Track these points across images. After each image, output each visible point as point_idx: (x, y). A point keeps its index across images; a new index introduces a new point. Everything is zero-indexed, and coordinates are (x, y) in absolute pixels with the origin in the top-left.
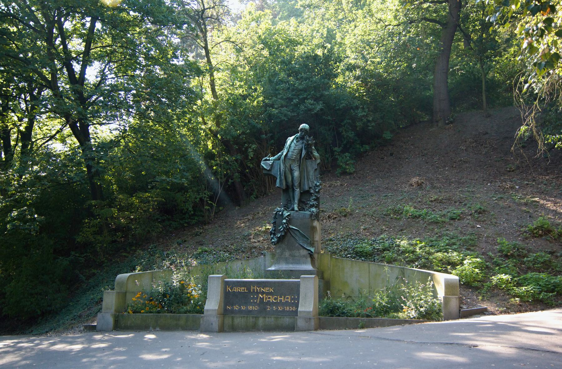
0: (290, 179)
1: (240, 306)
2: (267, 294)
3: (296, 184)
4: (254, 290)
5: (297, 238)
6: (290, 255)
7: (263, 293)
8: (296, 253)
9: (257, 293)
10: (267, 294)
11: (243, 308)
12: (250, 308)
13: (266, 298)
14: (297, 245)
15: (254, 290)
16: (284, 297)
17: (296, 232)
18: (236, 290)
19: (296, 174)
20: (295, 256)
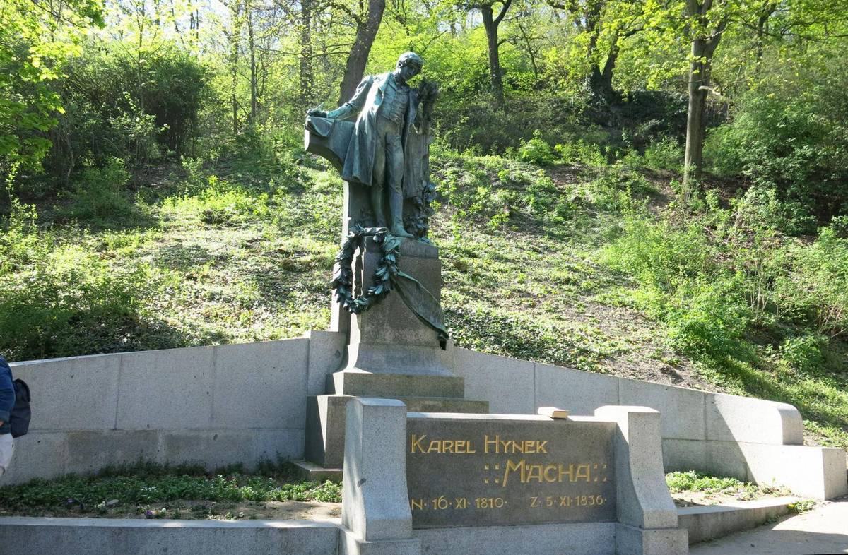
0: (383, 165)
1: (452, 497)
2: (531, 459)
3: (397, 177)
4: (492, 447)
5: (412, 300)
6: (395, 339)
7: (517, 456)
8: (410, 336)
9: (503, 456)
10: (531, 459)
11: (462, 504)
12: (480, 502)
13: (527, 472)
14: (412, 316)
15: (492, 447)
16: (575, 468)
17: (410, 287)
18: (440, 447)
19: (399, 156)
20: (406, 343)
